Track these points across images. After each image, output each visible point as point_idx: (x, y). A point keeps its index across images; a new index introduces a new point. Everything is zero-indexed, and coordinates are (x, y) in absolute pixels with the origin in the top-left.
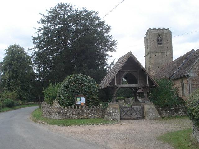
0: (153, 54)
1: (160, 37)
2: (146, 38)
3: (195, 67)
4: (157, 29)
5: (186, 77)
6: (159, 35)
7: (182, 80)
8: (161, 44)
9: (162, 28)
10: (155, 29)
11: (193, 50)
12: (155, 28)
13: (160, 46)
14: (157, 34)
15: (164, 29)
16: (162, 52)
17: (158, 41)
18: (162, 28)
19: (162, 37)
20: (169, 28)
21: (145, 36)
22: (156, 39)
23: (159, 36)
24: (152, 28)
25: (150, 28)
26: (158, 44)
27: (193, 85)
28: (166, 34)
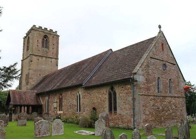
0: (34, 58)
1: (45, 39)
2: (27, 37)
3: (143, 67)
4: (43, 28)
5: (128, 81)
6: (45, 37)
7: (112, 89)
8: (46, 47)
9: (48, 29)
10: (40, 27)
11: (111, 50)
12: (41, 27)
14: (44, 34)
15: (51, 30)
17: (43, 42)
18: (48, 29)
19: (48, 39)
20: (41, 41)
21: (25, 35)
22: (40, 40)
23: (45, 38)
24: (37, 27)
25: (34, 26)
26: (43, 46)
27: (141, 95)
28: (53, 37)
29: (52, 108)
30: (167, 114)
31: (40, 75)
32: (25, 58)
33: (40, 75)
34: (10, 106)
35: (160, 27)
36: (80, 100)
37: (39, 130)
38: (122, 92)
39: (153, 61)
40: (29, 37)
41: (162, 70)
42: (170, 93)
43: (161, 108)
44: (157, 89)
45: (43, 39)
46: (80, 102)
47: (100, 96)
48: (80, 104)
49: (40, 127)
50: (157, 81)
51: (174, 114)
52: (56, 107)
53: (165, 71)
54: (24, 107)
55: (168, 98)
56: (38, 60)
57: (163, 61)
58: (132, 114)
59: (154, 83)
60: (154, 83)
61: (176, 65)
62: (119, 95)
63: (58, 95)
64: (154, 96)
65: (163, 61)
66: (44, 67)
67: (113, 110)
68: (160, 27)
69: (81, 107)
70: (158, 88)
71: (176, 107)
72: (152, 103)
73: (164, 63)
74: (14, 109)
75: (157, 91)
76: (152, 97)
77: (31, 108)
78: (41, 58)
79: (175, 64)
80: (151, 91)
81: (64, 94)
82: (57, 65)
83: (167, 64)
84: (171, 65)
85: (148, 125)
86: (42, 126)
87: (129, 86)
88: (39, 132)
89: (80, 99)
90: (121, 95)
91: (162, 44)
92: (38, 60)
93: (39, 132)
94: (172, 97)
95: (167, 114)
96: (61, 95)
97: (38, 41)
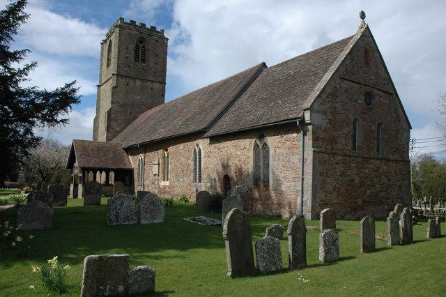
2: (108, 42)
4: (138, 24)
6: (141, 41)
8: (143, 61)
9: (148, 26)
10: (133, 23)
11: (264, 65)
13: (141, 65)
16: (143, 80)
17: (137, 50)
19: (146, 45)
22: (132, 47)
23: (141, 42)
26: (136, 59)
28: (156, 41)
29: (151, 175)
30: (369, 192)
31: (131, 113)
32: (103, 81)
33: (131, 113)
34: (76, 171)
35: (363, 15)
36: (200, 160)
37: (117, 213)
38: (280, 145)
39: (345, 85)
40: (111, 41)
41: (364, 103)
42: (378, 151)
43: (357, 181)
44: (351, 141)
45: (137, 45)
46: (200, 163)
47: (239, 153)
48: (200, 169)
49: (119, 207)
50: (352, 126)
51: (384, 193)
52: (157, 173)
53: (370, 106)
54: (101, 173)
55: (373, 161)
56: (128, 85)
57: (366, 85)
58: (300, 189)
59: (345, 130)
60: (345, 130)
61: (394, 95)
62: (275, 150)
63: (161, 151)
64: (344, 156)
65: (366, 85)
66: (138, 98)
67: (197, 151)
68: (363, 15)
69: (202, 173)
70: (354, 141)
71: (389, 180)
72: (340, 169)
73: (369, 89)
74: (81, 175)
75: (350, 146)
76: (340, 158)
77: (112, 175)
78: (132, 81)
79: (391, 94)
80: (339, 146)
81: (171, 149)
82: (163, 96)
83: (375, 91)
84: (382, 94)
85: (327, 211)
86: (121, 205)
87: (295, 135)
88: (117, 217)
89: (200, 158)
90: (278, 151)
91: (366, 51)
92: (128, 85)
93: (117, 217)
94: (381, 159)
95: (369, 192)
96: (167, 150)
97: (127, 48)
